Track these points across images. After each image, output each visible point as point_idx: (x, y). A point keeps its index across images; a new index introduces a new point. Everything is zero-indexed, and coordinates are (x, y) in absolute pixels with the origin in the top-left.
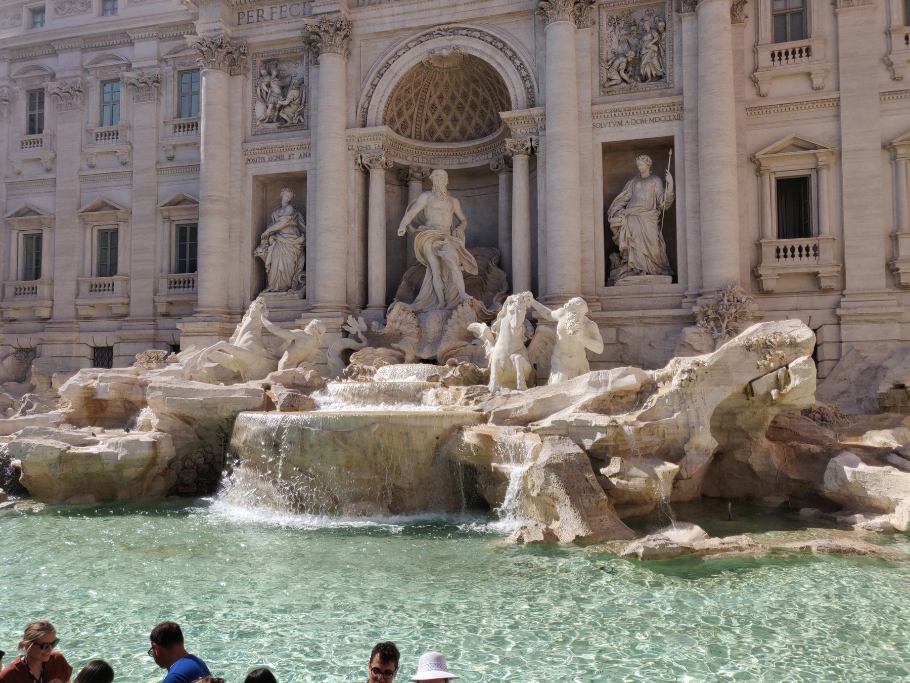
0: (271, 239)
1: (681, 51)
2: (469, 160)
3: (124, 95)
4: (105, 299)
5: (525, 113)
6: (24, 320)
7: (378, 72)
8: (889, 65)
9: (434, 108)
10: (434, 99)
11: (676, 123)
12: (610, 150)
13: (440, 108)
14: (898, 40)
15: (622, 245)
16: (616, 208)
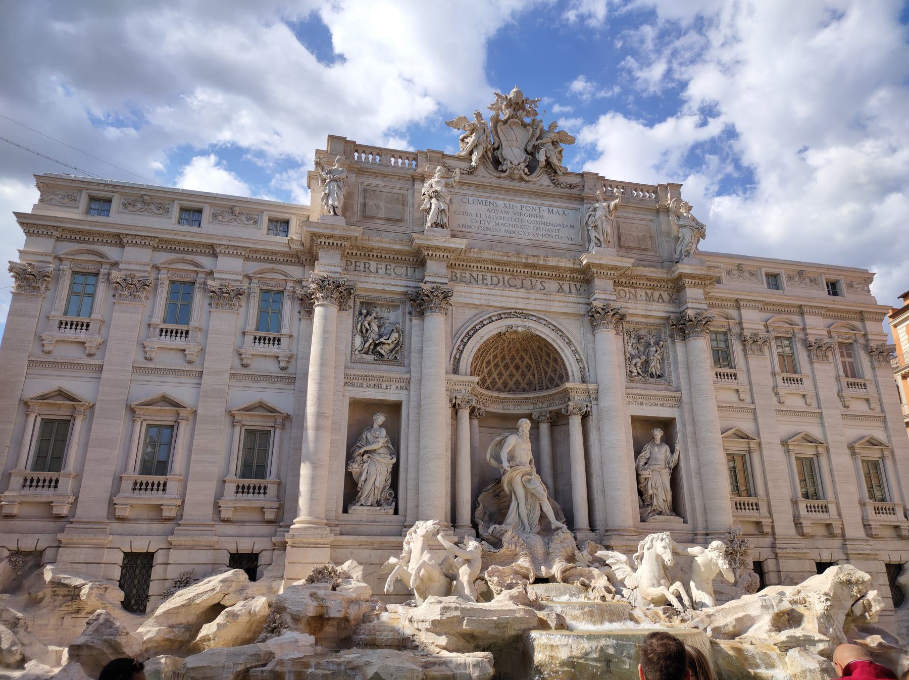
0: (365, 457)
1: (676, 363)
2: (511, 407)
3: (199, 299)
4: (155, 497)
5: (584, 386)
6: (25, 518)
7: (468, 333)
8: (777, 394)
9: (488, 363)
10: (491, 358)
11: (676, 409)
12: (635, 419)
13: (492, 364)
14: (779, 379)
15: (650, 492)
16: (642, 463)
